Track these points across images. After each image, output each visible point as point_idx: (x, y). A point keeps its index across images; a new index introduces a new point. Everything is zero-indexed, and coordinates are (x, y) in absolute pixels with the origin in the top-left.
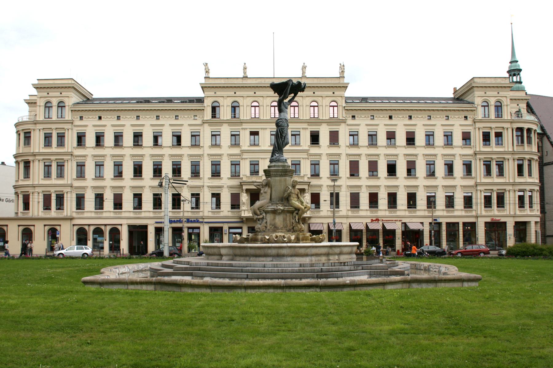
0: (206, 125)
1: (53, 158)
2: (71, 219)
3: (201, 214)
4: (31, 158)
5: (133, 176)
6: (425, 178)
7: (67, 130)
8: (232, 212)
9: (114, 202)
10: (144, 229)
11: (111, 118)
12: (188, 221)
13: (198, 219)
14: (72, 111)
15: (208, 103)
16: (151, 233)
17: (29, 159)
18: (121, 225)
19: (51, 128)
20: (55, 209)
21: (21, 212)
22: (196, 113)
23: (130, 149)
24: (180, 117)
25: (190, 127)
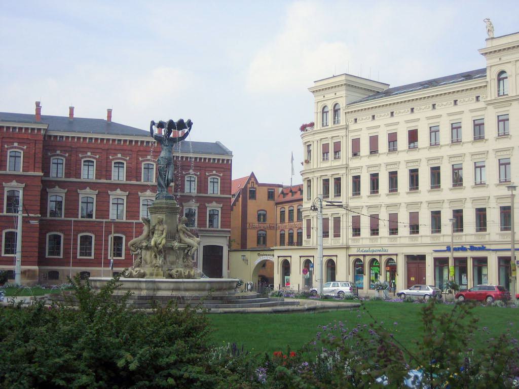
0: (490, 108)
1: (329, 173)
2: (348, 248)
3: (487, 238)
4: (310, 176)
5: (409, 189)
6: (429, 191)
7: (342, 138)
8: (500, 234)
9: (371, 227)
10: (422, 258)
11: (404, 112)
12: (473, 248)
13: (485, 246)
14: (346, 113)
15: (492, 75)
16: (429, 266)
17: (308, 178)
18: (397, 255)
19: (339, 136)
20: (500, 229)
21: (305, 241)
22: (477, 92)
23: (405, 153)
24: (460, 102)
25: (387, 127)
